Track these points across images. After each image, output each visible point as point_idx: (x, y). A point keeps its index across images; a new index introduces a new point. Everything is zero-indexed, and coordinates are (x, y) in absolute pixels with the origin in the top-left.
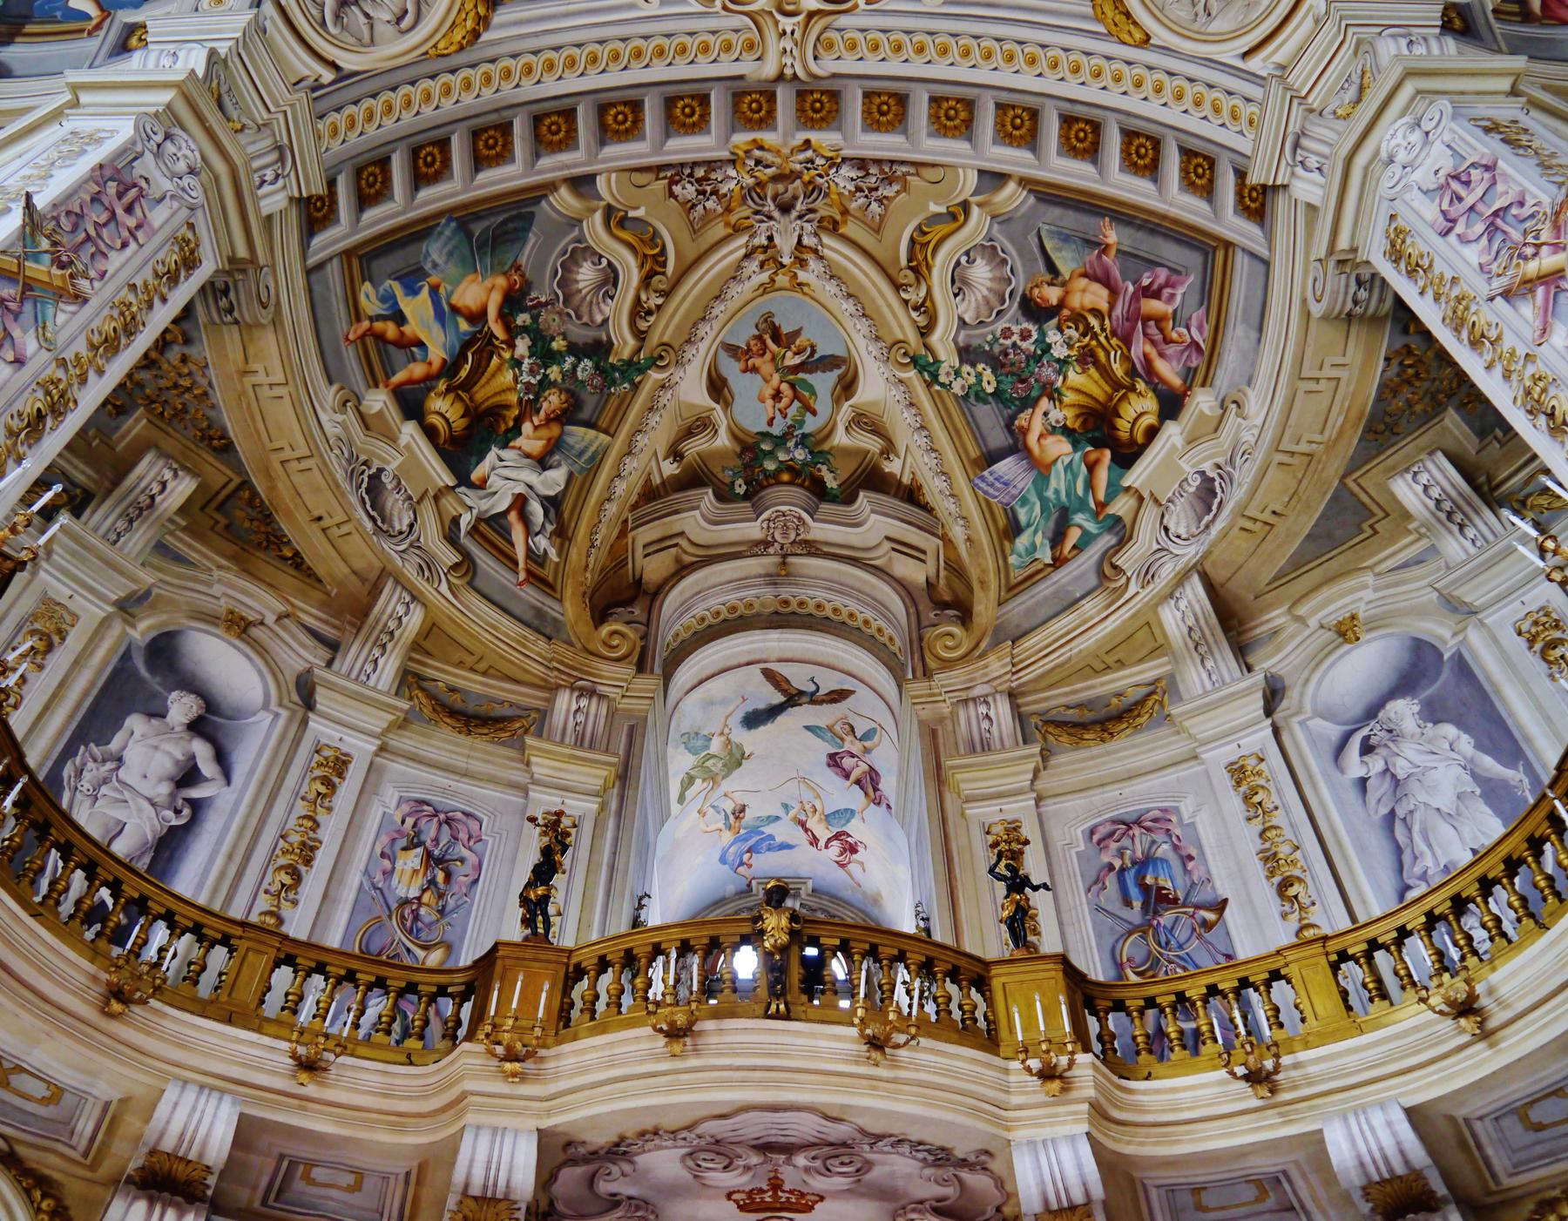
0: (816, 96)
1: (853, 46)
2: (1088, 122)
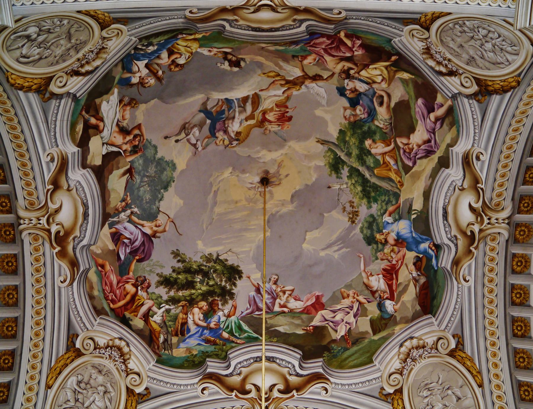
0: (12, 232)
1: (36, 250)
2: (13, 363)
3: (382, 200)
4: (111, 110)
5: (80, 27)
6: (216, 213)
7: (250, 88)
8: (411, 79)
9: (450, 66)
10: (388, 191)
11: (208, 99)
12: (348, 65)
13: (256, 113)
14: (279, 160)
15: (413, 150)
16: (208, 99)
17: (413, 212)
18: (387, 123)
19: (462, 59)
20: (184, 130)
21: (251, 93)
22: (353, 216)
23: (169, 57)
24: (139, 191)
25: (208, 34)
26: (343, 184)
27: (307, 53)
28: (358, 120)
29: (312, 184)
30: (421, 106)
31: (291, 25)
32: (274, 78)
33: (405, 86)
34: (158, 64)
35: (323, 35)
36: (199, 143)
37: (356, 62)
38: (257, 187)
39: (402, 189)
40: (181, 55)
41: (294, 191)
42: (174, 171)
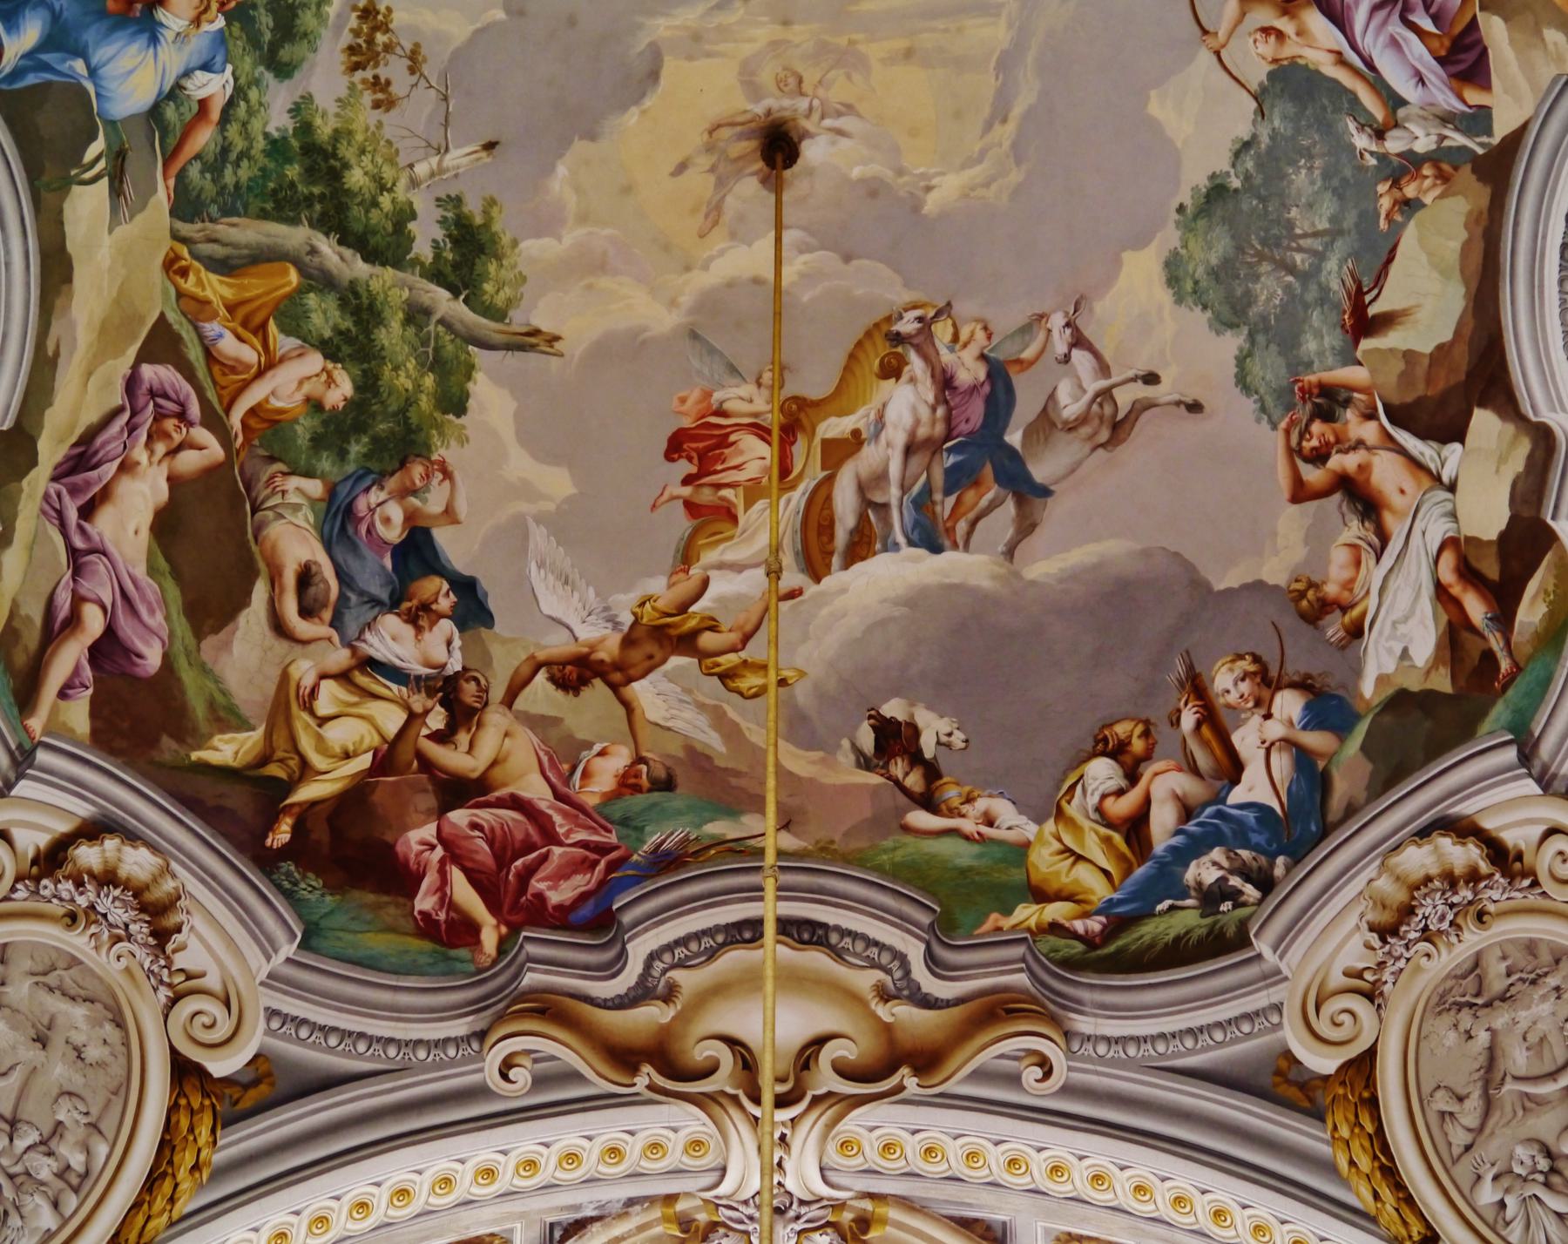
3: (249, 158)
4: (1397, 614)
5: (1442, 1114)
6: (1003, 22)
7: (839, 602)
8: (202, 742)
9: (67, 887)
10: (228, 211)
11: (1010, 553)
12: (456, 759)
13: (817, 473)
14: (718, 240)
15: (150, 437)
16: (1010, 553)
17: (102, 164)
18: (269, 504)
19: (28, 964)
20: (1120, 416)
21: (836, 579)
22: (370, 41)
23: (1147, 801)
24: (1332, 220)
25: (994, 919)
26: (432, 175)
27: (617, 810)
28: (392, 474)
29: (571, 142)
30: (147, 643)
31: (681, 965)
32: (745, 662)
33: (220, 699)
34: (1194, 770)
35: (561, 919)
36: (1060, 346)
37: (424, 776)
38: (816, 116)
39: (167, 243)
40: (1099, 809)
41: (648, 103)
42: (1175, 254)
